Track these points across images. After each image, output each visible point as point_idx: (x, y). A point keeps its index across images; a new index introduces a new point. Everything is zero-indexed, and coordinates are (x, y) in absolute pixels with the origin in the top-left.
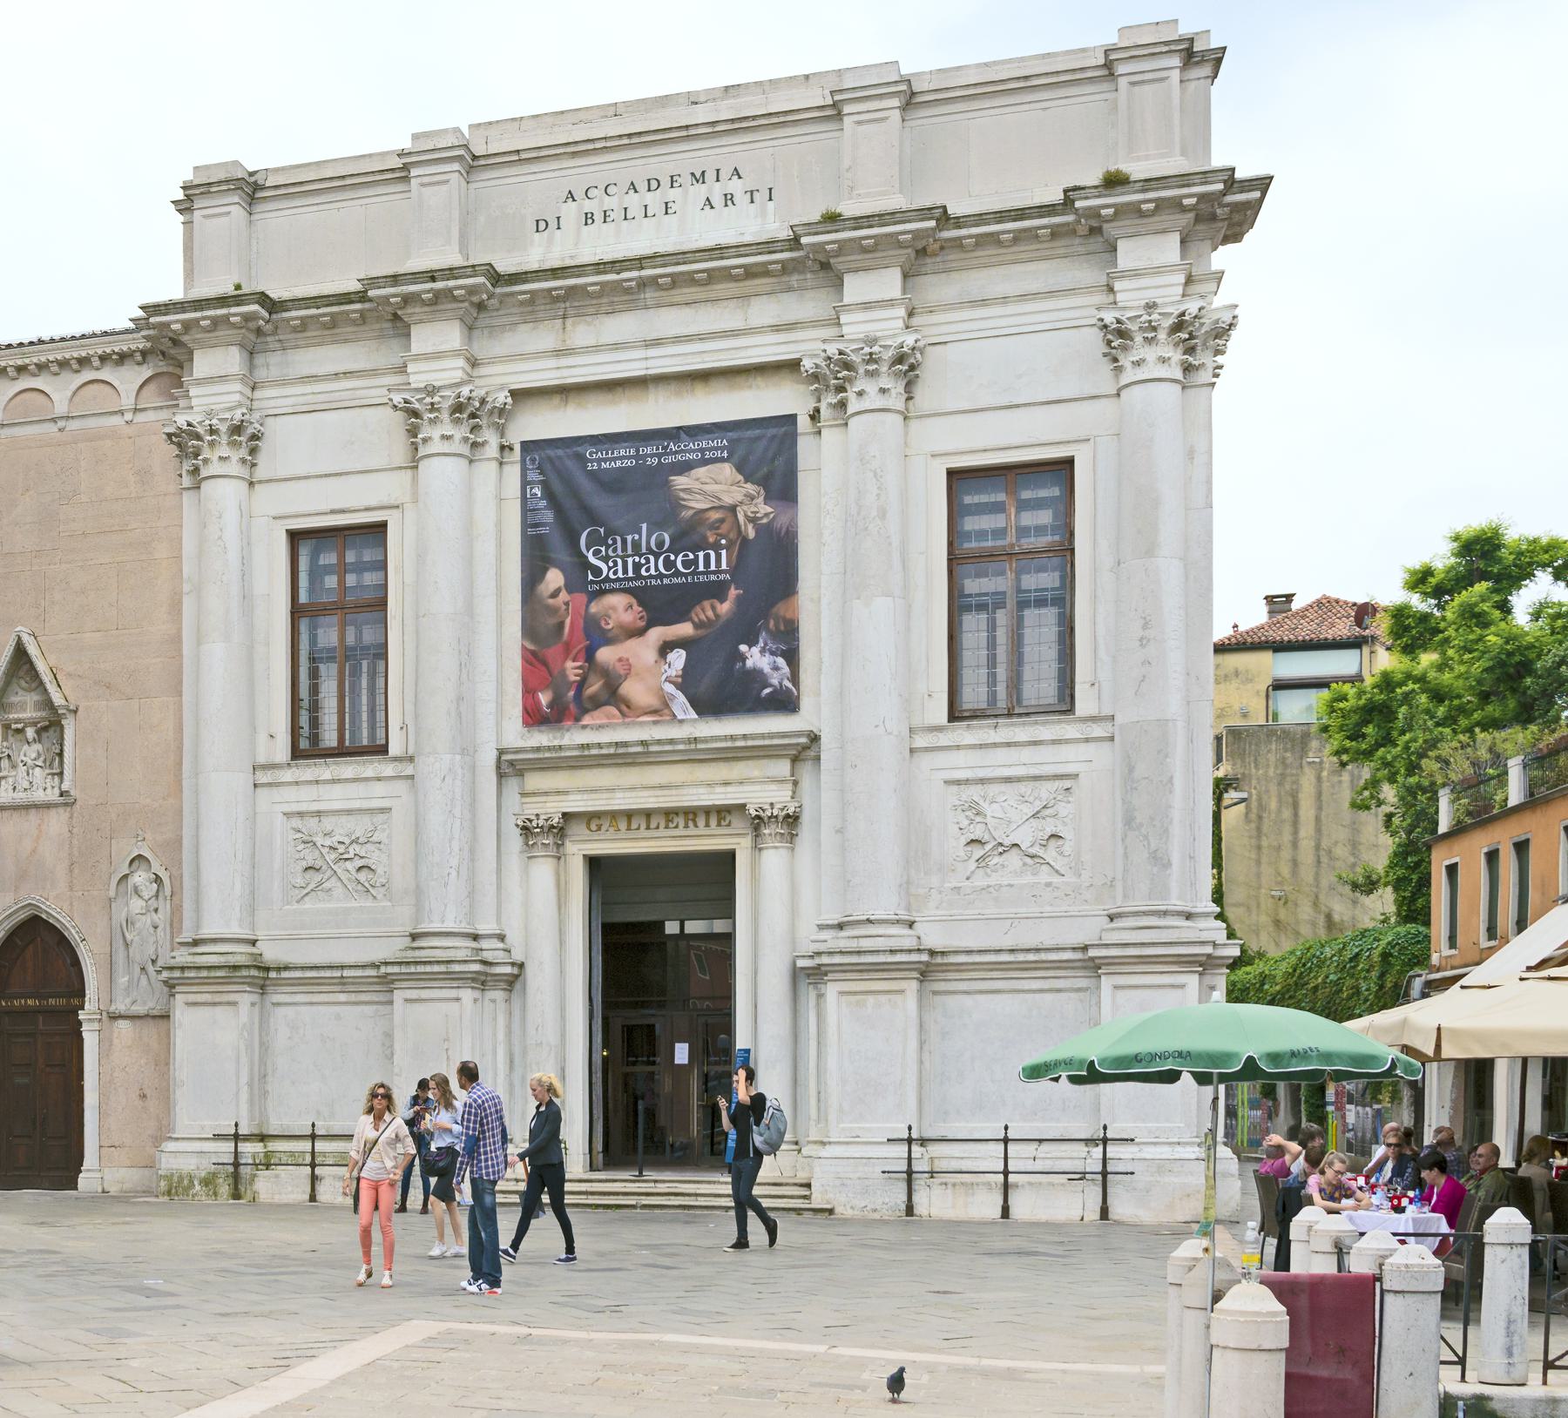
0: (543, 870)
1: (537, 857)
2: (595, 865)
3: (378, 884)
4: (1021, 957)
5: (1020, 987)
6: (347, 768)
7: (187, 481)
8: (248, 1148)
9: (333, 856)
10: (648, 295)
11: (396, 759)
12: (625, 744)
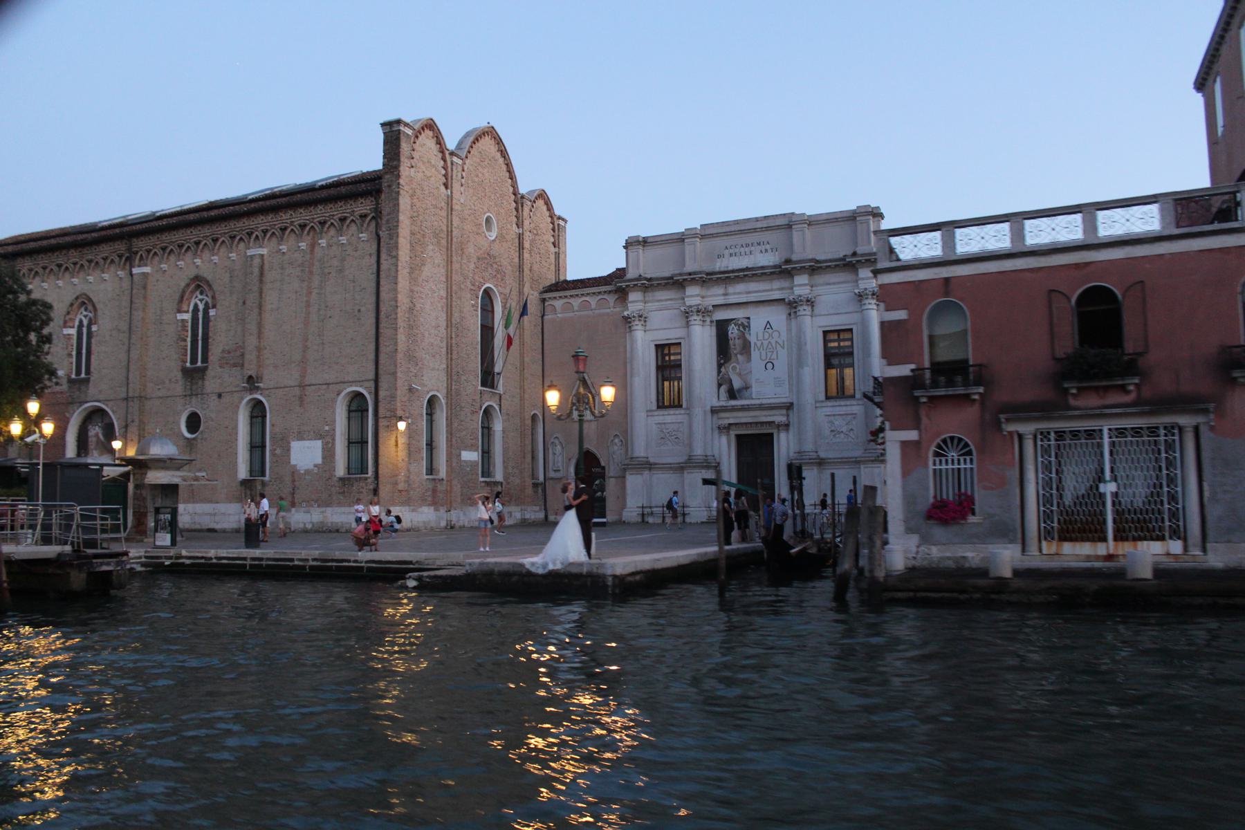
0: (724, 439)
6: (672, 411)
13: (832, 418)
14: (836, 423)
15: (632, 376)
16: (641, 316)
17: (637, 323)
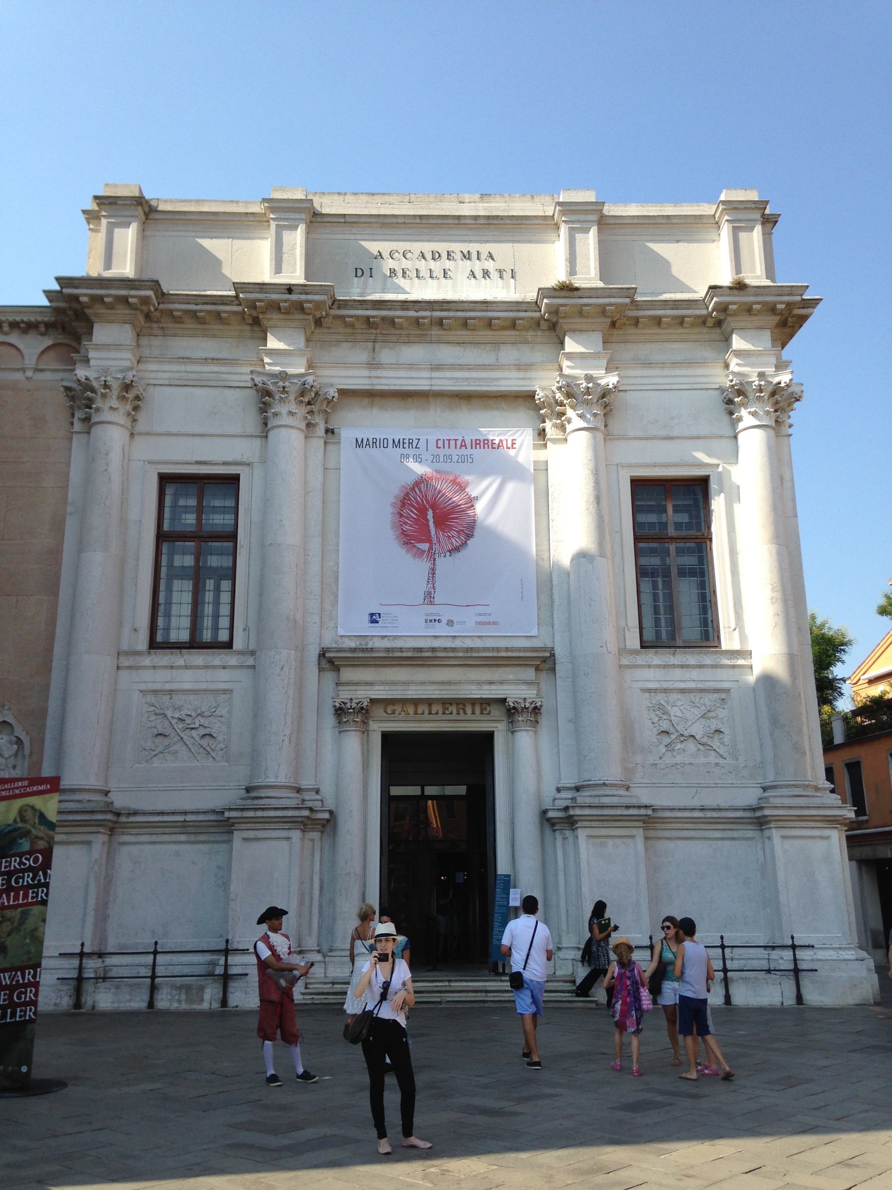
0: (352, 742)
1: (350, 731)
2: (387, 738)
3: (218, 749)
4: (709, 814)
5: (707, 836)
6: (198, 658)
7: (78, 426)
8: (92, 965)
9: (180, 726)
10: (433, 332)
11: (240, 653)
12: (420, 650)
13: (661, 698)
14: (675, 712)
15: (81, 547)
16: (127, 387)
17: (114, 403)
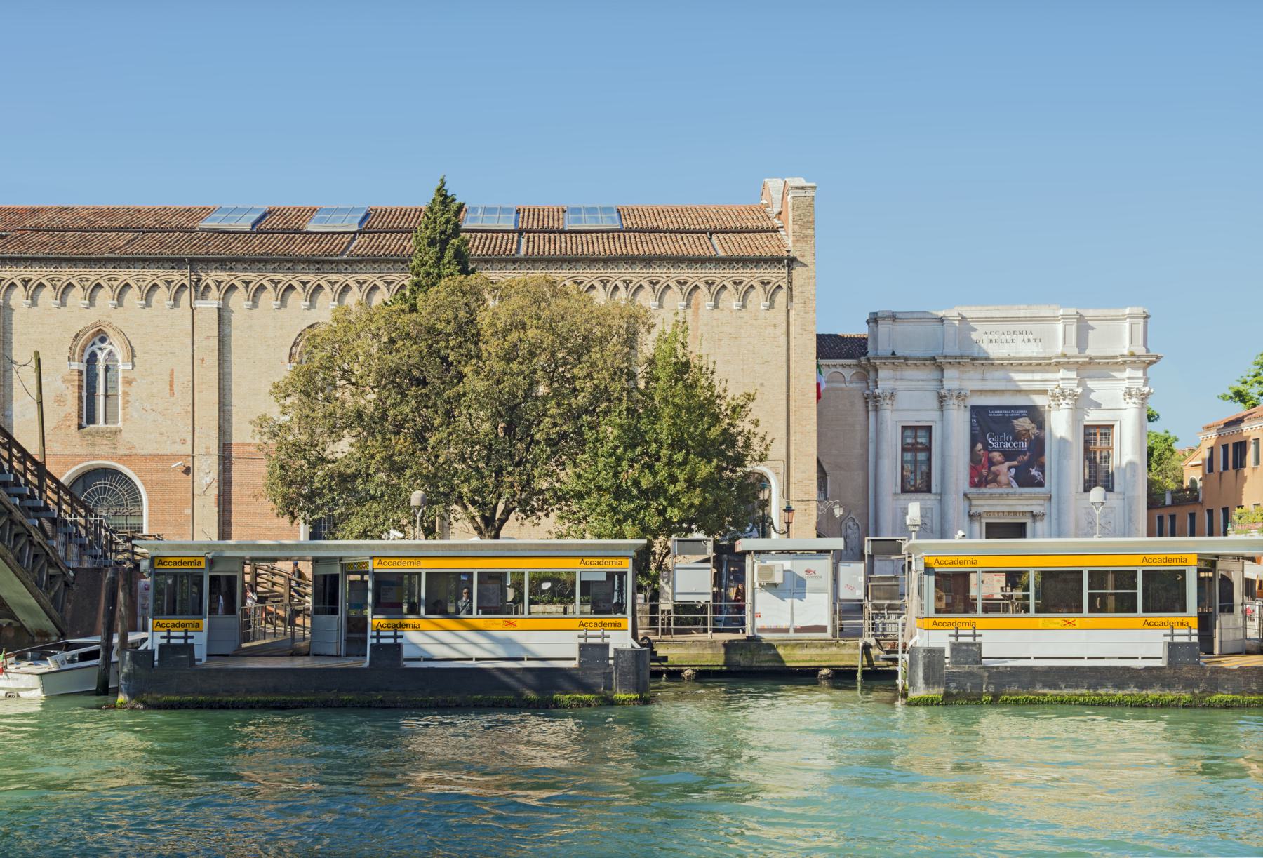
2: (988, 525)
11: (935, 494)
17: (887, 401)
